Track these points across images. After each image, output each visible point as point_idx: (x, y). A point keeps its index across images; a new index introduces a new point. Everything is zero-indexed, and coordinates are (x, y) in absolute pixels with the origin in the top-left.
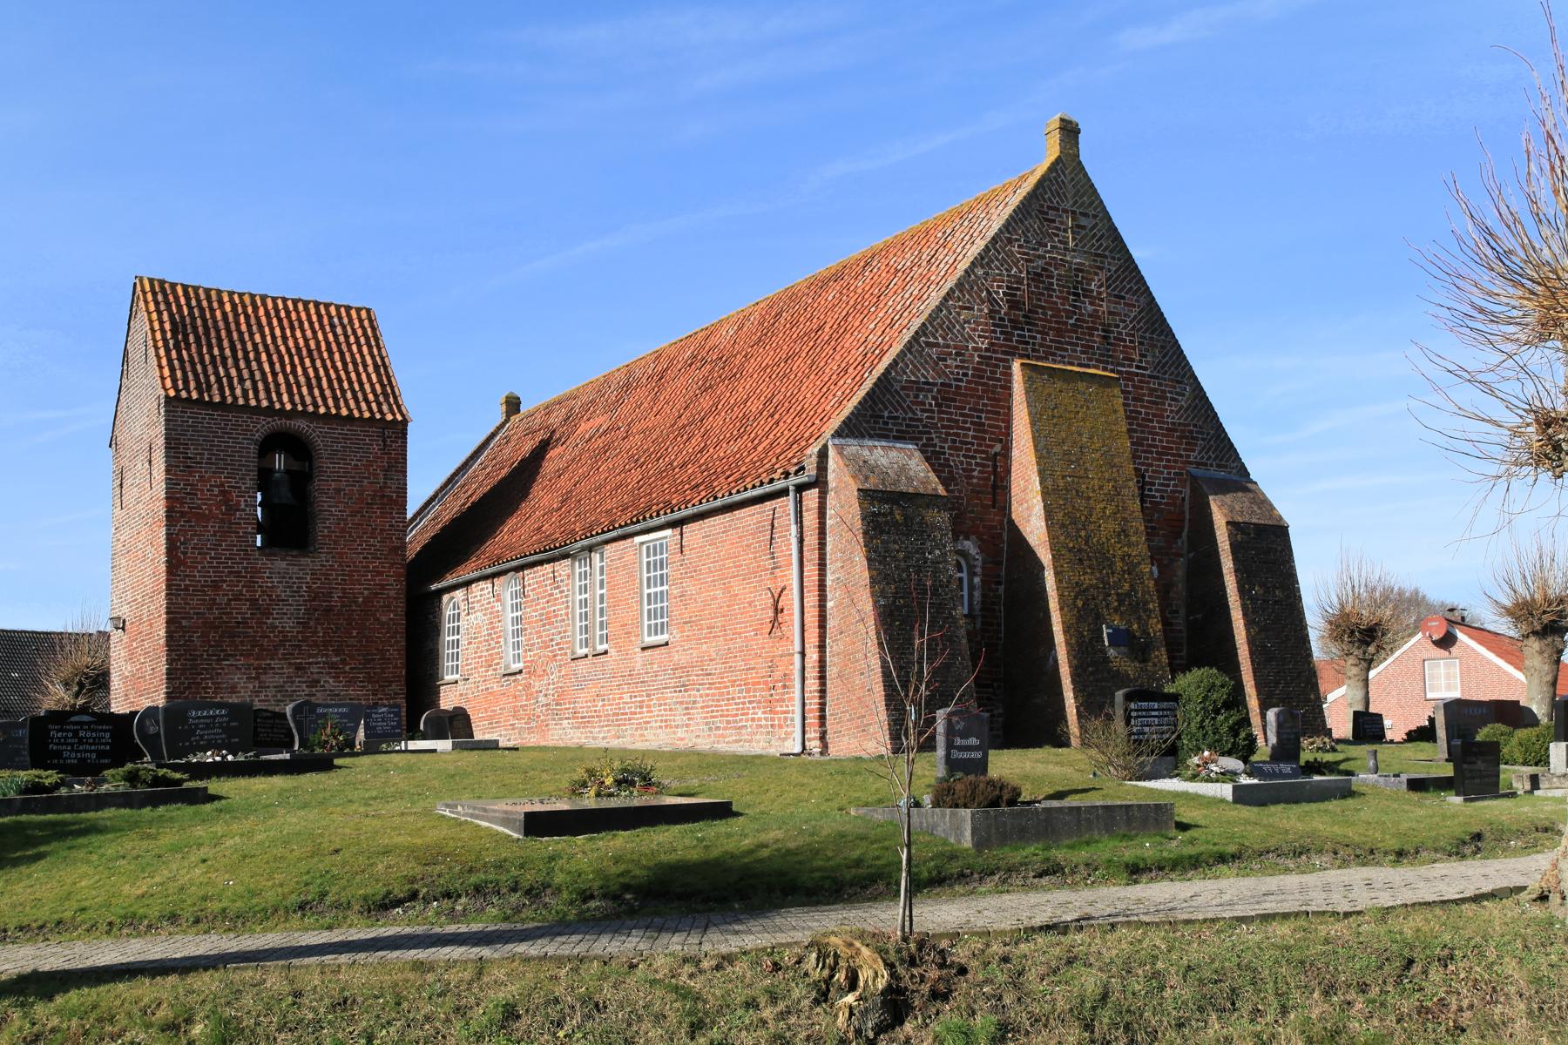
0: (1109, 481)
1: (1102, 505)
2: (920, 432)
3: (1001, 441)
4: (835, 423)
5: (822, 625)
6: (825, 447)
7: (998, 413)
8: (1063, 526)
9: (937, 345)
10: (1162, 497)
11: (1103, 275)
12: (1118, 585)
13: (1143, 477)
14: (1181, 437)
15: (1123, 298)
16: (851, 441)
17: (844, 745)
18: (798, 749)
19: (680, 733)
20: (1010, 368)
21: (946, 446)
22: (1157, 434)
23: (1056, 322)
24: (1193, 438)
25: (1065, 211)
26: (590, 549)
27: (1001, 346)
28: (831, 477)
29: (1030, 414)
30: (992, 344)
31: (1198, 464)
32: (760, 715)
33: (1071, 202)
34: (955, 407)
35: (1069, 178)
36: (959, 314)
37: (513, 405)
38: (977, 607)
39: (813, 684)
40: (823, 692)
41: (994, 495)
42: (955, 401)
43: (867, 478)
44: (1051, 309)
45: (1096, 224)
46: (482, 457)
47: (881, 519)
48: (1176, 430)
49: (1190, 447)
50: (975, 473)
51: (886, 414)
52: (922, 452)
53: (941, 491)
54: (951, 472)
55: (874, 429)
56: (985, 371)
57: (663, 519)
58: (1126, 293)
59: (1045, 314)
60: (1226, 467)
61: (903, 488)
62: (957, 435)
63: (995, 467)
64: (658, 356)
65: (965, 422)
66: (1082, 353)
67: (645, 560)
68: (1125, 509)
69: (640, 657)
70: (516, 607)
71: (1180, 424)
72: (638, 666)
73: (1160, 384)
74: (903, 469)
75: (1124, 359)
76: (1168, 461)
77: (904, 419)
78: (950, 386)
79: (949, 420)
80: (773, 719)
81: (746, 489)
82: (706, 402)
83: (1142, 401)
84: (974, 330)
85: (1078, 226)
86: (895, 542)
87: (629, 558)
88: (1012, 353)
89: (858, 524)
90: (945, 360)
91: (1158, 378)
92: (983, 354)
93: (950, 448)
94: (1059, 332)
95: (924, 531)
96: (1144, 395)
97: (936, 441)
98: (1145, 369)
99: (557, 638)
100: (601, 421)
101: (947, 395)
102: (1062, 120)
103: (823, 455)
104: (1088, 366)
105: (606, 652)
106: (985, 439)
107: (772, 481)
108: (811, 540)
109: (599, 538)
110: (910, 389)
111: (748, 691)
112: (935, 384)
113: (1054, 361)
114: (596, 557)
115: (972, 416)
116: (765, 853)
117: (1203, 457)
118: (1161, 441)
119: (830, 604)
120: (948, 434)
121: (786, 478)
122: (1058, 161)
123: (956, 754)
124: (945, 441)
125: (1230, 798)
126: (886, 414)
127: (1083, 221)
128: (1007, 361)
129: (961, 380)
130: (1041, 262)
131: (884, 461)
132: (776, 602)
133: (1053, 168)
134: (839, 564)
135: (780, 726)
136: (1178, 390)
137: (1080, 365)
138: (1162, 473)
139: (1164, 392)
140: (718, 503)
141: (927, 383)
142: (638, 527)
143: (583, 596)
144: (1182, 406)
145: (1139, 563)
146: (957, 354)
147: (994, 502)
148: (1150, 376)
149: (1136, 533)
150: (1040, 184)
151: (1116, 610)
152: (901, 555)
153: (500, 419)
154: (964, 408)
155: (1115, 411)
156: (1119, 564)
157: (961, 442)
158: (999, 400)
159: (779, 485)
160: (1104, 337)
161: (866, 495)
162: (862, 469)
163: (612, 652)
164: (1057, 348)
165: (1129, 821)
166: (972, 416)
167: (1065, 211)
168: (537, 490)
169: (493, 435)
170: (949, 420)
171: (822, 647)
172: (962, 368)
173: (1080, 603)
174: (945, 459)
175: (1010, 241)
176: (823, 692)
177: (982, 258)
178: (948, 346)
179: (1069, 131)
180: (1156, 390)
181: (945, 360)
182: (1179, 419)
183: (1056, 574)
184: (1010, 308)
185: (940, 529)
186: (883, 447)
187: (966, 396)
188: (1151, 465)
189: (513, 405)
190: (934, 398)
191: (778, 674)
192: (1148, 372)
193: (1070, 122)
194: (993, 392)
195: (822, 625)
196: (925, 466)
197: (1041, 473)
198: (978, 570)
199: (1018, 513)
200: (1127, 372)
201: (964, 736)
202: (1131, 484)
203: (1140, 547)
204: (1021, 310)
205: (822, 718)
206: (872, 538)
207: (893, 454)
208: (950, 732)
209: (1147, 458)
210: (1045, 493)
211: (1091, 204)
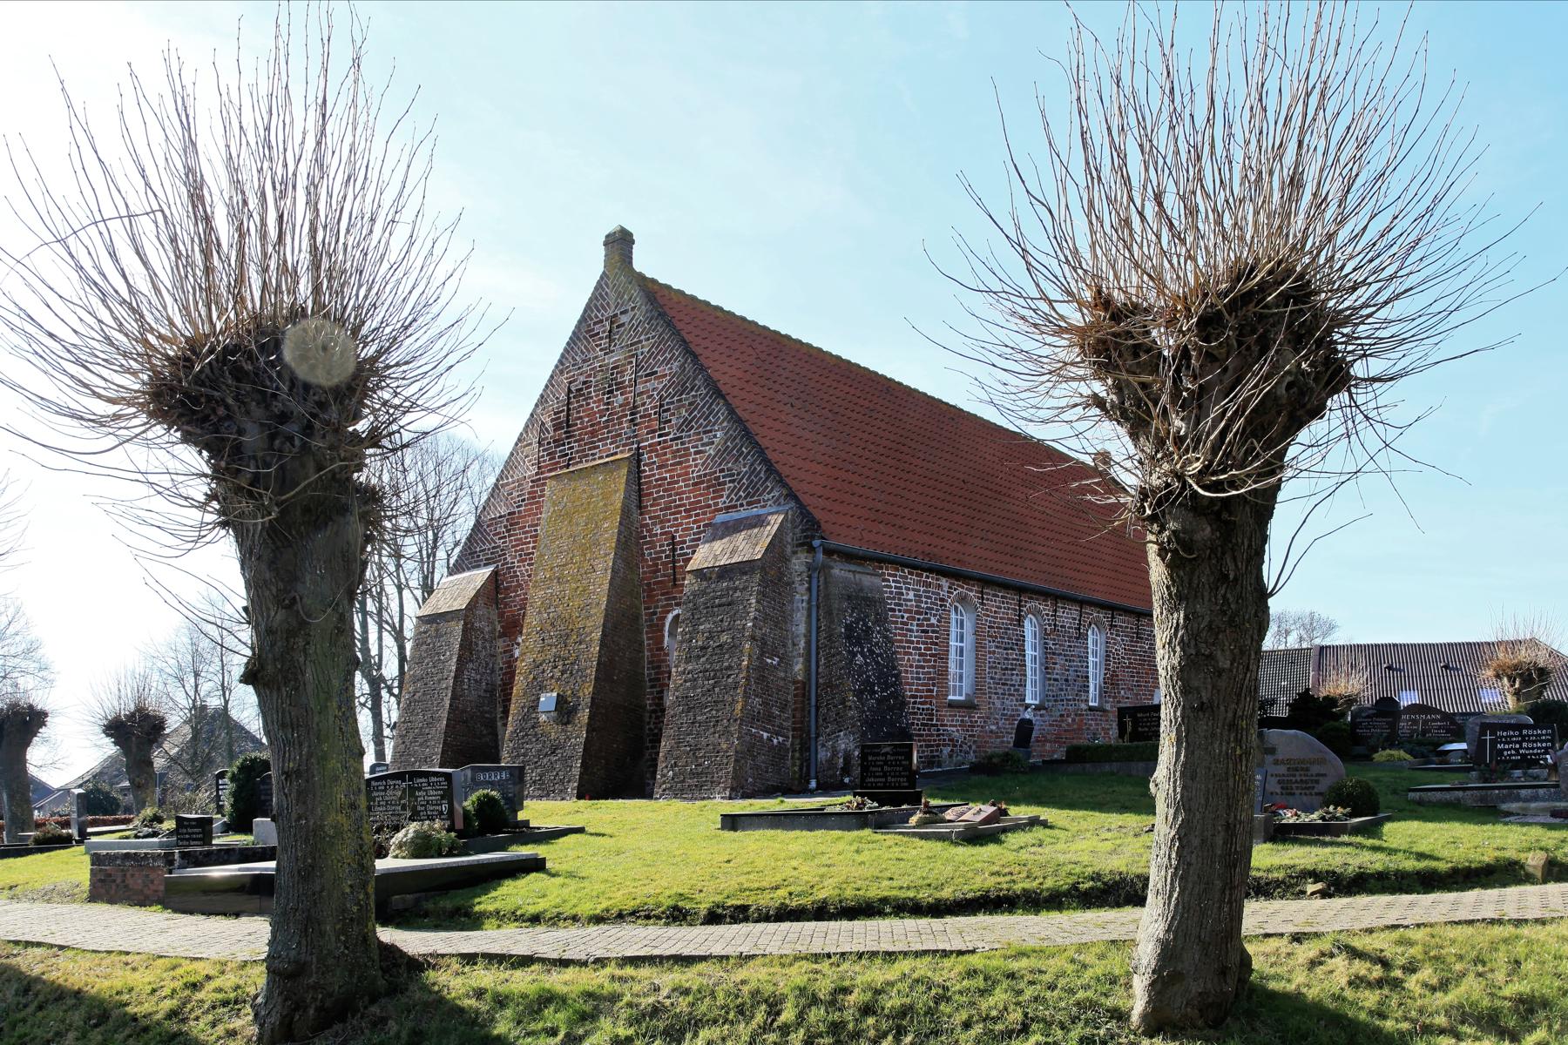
13: (673, 538)
22: (684, 493)
24: (719, 484)
31: (727, 508)
33: (613, 308)
42: (518, 523)
48: (703, 482)
51: (478, 549)
54: (518, 581)
60: (759, 501)
62: (522, 550)
65: (526, 538)
71: (705, 475)
73: (682, 444)
75: (647, 434)
76: (697, 515)
77: (489, 549)
79: (515, 540)
83: (667, 466)
91: (681, 438)
96: (668, 460)
104: (616, 453)
118: (688, 498)
136: (705, 440)
137: (607, 456)
138: (692, 529)
139: (688, 449)
144: (710, 455)
148: (672, 440)
170: (515, 540)
179: (620, 243)
180: (678, 450)
188: (681, 524)
192: (671, 436)
200: (650, 445)
209: (676, 519)
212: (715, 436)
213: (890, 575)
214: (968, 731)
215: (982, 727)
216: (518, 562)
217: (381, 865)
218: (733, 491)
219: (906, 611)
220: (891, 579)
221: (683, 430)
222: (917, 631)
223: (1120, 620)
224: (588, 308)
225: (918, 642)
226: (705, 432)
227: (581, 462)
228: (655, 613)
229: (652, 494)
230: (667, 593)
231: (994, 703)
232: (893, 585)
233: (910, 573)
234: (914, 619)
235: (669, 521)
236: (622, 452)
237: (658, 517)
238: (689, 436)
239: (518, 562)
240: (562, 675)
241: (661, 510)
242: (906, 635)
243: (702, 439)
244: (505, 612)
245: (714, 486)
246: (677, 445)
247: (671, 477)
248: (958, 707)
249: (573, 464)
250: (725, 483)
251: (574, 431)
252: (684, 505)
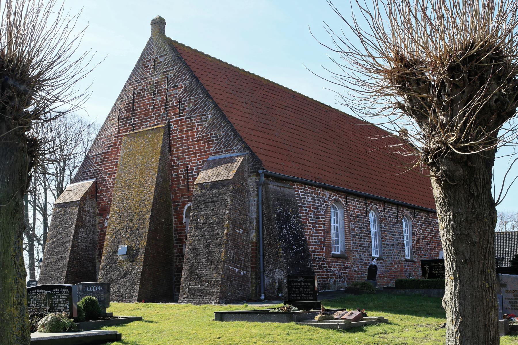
2: (98, 174)
13: (187, 167)
21: (106, 176)
22: (192, 145)
24: (210, 141)
30: (119, 131)
33: (156, 54)
35: (155, 44)
42: (108, 158)
48: (202, 140)
51: (87, 170)
54: (107, 187)
56: (117, 142)
58: (179, 83)
60: (230, 150)
62: (110, 171)
65: (112, 165)
71: (203, 136)
73: (191, 120)
75: (174, 115)
76: (199, 156)
77: (93, 170)
79: (106, 166)
91: (190, 118)
92: (116, 135)
96: (184, 128)
104: (158, 124)
117: (217, 149)
118: (195, 147)
124: (106, 175)
136: (203, 119)
137: (153, 126)
138: (197, 163)
139: (194, 123)
144: (205, 126)
148: (186, 119)
154: (111, 160)
157: (111, 174)
170: (106, 166)
180: (189, 124)
182: (203, 134)
188: (191, 160)
192: (185, 117)
200: (175, 121)
209: (189, 158)
212: (208, 117)
213: (299, 188)
214: (343, 270)
215: (350, 268)
216: (108, 177)
217: (34, 336)
218: (217, 144)
219: (307, 207)
220: (299, 190)
221: (191, 114)
222: (314, 217)
223: (419, 214)
224: (143, 54)
225: (315, 223)
226: (202, 115)
227: (140, 128)
228: (178, 205)
229: (176, 145)
230: (184, 195)
231: (355, 256)
232: (300, 193)
233: (309, 188)
234: (312, 211)
235: (185, 158)
236: (161, 124)
237: (179, 156)
238: (195, 117)
239: (108, 177)
240: (130, 236)
241: (181, 153)
242: (308, 220)
243: (201, 119)
244: (100, 203)
245: (208, 142)
246: (188, 121)
247: (186, 137)
248: (337, 258)
249: (136, 129)
250: (213, 141)
251: (136, 113)
252: (192, 151)
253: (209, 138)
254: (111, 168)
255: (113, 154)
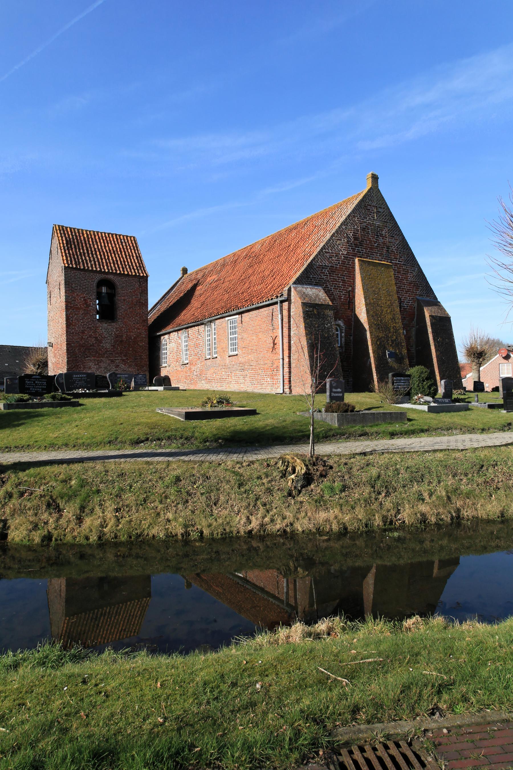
0: (389, 301)
1: (386, 309)
3: (351, 286)
4: (294, 279)
5: (290, 349)
6: (290, 287)
7: (350, 277)
8: (373, 316)
9: (329, 253)
10: (407, 307)
11: (386, 229)
12: (391, 337)
13: (401, 299)
14: (414, 286)
15: (394, 237)
16: (299, 286)
17: (297, 390)
18: (281, 392)
19: (242, 386)
20: (354, 261)
23: (371, 245)
25: (373, 206)
26: (211, 322)
27: (351, 253)
28: (292, 298)
29: (361, 277)
30: (348, 253)
31: (420, 295)
32: (269, 380)
34: (336, 274)
36: (336, 242)
37: (185, 271)
38: (343, 344)
39: (286, 370)
40: (290, 372)
41: (349, 305)
42: (335, 272)
43: (304, 299)
44: (369, 240)
45: (384, 211)
46: (174, 289)
47: (309, 313)
49: (417, 289)
50: (342, 297)
52: (324, 290)
53: (330, 303)
54: (334, 297)
55: (307, 281)
57: (235, 312)
59: (366, 242)
60: (429, 296)
61: (317, 302)
62: (336, 284)
63: (349, 295)
64: (234, 254)
66: (379, 256)
67: (229, 326)
68: (394, 311)
69: (228, 360)
70: (186, 341)
72: (227, 362)
74: (317, 295)
78: (333, 267)
79: (333, 279)
80: (273, 381)
81: (263, 302)
82: (250, 271)
84: (342, 247)
85: (378, 212)
86: (314, 321)
87: (224, 325)
88: (355, 256)
89: (302, 314)
90: (332, 258)
93: (334, 289)
94: (371, 249)
95: (324, 317)
97: (329, 286)
98: (401, 262)
99: (200, 352)
100: (215, 277)
101: (332, 270)
102: (372, 174)
103: (289, 290)
104: (381, 261)
105: (216, 357)
106: (345, 285)
107: (272, 299)
108: (286, 320)
109: (214, 318)
110: (320, 268)
111: (265, 371)
112: (328, 266)
113: (370, 259)
114: (213, 324)
115: (341, 278)
116: (268, 428)
119: (292, 342)
120: (333, 284)
121: (277, 298)
122: (371, 188)
123: (333, 394)
124: (332, 286)
125: (427, 410)
126: (311, 276)
127: (380, 210)
128: (353, 258)
129: (337, 265)
130: (365, 224)
131: (310, 293)
132: (274, 341)
133: (369, 191)
134: (295, 328)
135: (276, 384)
137: (378, 260)
139: (408, 270)
140: (254, 306)
141: (326, 266)
142: (227, 314)
143: (209, 338)
145: (399, 329)
146: (336, 256)
147: (349, 307)
149: (398, 319)
150: (364, 197)
151: (391, 345)
152: (317, 325)
153: (180, 276)
155: (391, 277)
156: (392, 330)
158: (351, 272)
159: (275, 300)
160: (387, 251)
161: (304, 304)
162: (303, 295)
163: (219, 357)
164: (371, 254)
165: (391, 418)
166: (341, 278)
167: (373, 206)
168: (193, 301)
169: (178, 282)
170: (333, 279)
171: (290, 357)
172: (338, 261)
173: (378, 343)
174: (332, 293)
175: (354, 216)
176: (290, 372)
177: (345, 222)
178: (333, 253)
179: (375, 178)
180: (405, 269)
181: (332, 258)
183: (370, 333)
184: (354, 240)
185: (330, 316)
186: (310, 288)
187: (339, 270)
189: (185, 271)
190: (328, 271)
191: (275, 366)
193: (375, 175)
194: (349, 269)
195: (290, 349)
196: (325, 295)
197: (365, 298)
198: (344, 331)
199: (357, 311)
201: (336, 388)
202: (396, 302)
203: (399, 324)
204: (358, 240)
205: (290, 381)
206: (306, 319)
207: (314, 290)
208: (331, 387)
210: (367, 305)
211: (383, 204)
252: (405, 289)
253: (417, 284)
254: (338, 282)
255: (341, 271)
